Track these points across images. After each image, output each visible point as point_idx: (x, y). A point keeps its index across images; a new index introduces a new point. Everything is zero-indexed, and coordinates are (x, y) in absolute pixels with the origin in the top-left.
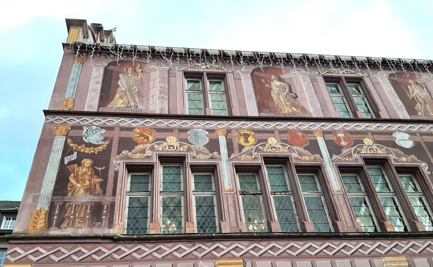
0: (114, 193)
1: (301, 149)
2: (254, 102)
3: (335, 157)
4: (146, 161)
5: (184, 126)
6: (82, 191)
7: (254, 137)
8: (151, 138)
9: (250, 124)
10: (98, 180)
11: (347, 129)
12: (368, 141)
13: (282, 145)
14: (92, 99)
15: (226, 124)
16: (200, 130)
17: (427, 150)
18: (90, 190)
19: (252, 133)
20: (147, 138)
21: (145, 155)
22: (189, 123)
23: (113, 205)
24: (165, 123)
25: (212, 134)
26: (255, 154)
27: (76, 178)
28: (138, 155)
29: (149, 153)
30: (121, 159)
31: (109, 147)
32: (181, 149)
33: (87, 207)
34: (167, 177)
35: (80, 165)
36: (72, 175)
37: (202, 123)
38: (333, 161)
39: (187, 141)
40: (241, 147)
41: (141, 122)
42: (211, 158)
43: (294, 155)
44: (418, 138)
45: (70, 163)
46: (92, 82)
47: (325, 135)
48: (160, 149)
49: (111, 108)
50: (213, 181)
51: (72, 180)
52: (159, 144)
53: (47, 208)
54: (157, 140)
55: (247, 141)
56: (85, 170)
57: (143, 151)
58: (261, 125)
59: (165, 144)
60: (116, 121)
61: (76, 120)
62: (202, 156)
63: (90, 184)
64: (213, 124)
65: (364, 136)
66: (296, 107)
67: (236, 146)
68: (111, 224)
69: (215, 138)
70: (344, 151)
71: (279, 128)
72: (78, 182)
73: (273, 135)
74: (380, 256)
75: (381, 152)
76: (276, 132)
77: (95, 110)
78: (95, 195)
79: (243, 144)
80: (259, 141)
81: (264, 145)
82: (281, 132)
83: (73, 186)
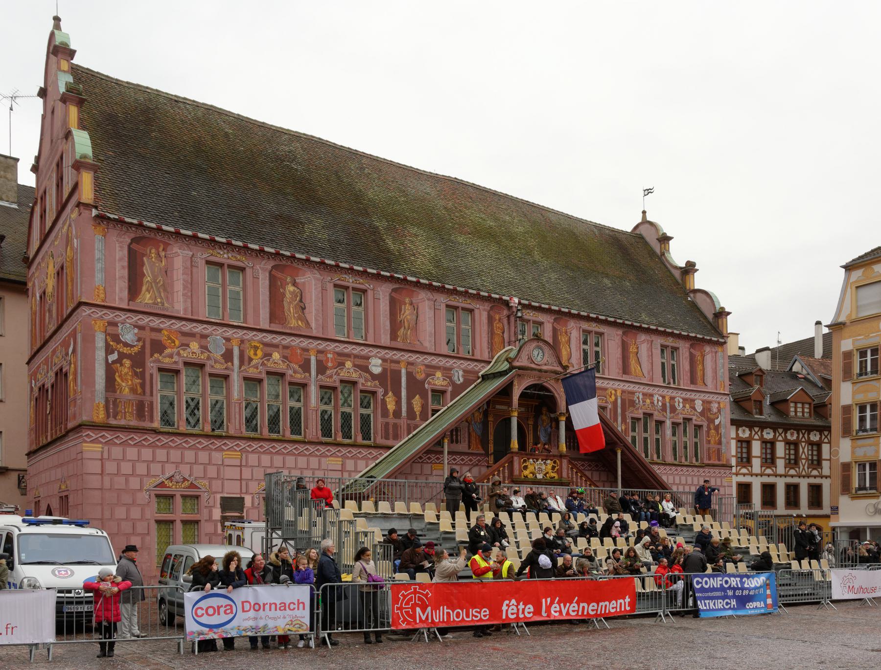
0: (152, 395)
1: (296, 367)
2: (268, 310)
3: (320, 376)
4: (174, 367)
5: (205, 332)
6: (127, 390)
7: (262, 351)
8: (177, 343)
9: (260, 335)
10: (138, 381)
11: (337, 350)
12: (349, 364)
13: (282, 361)
15: (241, 333)
16: (218, 337)
17: (389, 378)
18: (133, 390)
19: (261, 346)
20: (174, 342)
21: (173, 360)
22: (210, 329)
25: (228, 343)
27: (120, 376)
28: (167, 360)
29: (176, 358)
30: (154, 362)
32: (202, 357)
33: (133, 404)
34: (188, 378)
35: (122, 365)
36: (117, 374)
37: (221, 330)
38: (317, 381)
39: (206, 348)
40: (251, 360)
42: (226, 368)
43: (290, 372)
44: (388, 365)
45: (114, 362)
47: (318, 355)
48: (185, 355)
50: (224, 386)
51: (118, 379)
52: (184, 350)
53: (103, 402)
54: (182, 345)
55: (255, 354)
56: (126, 370)
57: (171, 356)
58: (269, 338)
59: (189, 350)
62: (218, 366)
63: (132, 384)
64: (230, 332)
65: (347, 359)
66: (302, 321)
67: (246, 358)
69: (230, 347)
70: (328, 372)
71: (284, 343)
72: (123, 382)
73: (277, 349)
75: (354, 376)
76: (280, 346)
78: (137, 394)
79: (252, 356)
81: (268, 360)
82: (285, 347)
83: (119, 385)
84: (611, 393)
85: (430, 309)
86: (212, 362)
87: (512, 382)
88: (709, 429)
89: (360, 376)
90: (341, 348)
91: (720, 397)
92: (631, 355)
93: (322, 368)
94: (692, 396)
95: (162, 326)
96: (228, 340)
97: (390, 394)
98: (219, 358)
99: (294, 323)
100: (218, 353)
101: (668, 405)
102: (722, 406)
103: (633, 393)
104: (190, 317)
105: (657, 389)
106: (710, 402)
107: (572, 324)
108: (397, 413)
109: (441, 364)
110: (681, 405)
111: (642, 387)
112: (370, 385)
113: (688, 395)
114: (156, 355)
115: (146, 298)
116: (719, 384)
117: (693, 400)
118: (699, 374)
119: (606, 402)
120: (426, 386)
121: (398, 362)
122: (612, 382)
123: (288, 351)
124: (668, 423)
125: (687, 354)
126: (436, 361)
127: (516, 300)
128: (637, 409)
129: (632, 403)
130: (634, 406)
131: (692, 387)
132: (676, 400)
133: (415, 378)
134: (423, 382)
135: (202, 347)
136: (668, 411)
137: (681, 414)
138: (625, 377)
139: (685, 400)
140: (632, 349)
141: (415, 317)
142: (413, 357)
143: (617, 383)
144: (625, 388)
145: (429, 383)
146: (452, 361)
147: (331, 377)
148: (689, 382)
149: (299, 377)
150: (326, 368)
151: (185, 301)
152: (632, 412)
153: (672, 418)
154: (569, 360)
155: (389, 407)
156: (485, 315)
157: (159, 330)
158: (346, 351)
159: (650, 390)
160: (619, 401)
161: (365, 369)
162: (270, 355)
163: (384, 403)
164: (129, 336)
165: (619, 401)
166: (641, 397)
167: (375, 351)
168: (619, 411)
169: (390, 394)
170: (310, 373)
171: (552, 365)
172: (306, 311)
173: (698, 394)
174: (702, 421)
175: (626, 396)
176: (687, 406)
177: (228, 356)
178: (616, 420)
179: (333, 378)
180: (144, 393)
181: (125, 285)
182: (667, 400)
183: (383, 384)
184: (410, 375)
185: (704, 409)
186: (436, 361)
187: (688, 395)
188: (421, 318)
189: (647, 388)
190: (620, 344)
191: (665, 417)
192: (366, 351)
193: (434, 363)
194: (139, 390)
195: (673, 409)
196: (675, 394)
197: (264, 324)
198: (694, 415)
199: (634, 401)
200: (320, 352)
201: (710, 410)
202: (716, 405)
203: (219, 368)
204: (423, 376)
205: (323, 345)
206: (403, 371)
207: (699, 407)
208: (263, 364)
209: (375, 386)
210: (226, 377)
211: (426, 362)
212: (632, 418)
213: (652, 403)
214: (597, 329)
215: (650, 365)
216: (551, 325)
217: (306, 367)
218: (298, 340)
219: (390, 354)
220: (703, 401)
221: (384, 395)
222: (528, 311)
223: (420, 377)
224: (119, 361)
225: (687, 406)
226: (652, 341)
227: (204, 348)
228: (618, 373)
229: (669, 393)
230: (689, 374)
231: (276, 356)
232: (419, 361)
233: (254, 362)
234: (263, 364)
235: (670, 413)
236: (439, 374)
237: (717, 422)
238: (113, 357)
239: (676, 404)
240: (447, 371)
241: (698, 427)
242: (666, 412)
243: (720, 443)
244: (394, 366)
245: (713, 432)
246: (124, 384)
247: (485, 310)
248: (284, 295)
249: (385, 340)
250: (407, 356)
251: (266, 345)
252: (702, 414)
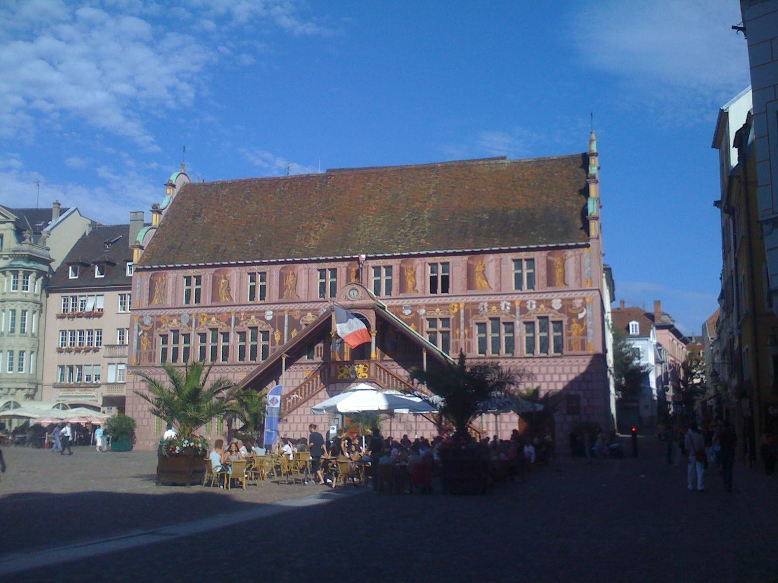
0: (155, 348)
1: (224, 324)
4: (166, 333)
5: (180, 313)
6: (145, 348)
8: (167, 321)
9: (206, 309)
11: (247, 310)
12: (253, 317)
14: (146, 300)
18: (148, 348)
23: (155, 353)
24: (172, 312)
26: (205, 327)
28: (162, 330)
31: (153, 326)
37: (187, 310)
39: (180, 321)
40: (201, 323)
41: (164, 311)
42: (189, 330)
44: (276, 314)
46: (145, 289)
49: (153, 305)
51: (142, 343)
55: (203, 320)
57: (164, 328)
58: (210, 310)
60: (155, 312)
61: (141, 313)
64: (192, 311)
68: (154, 362)
70: (241, 324)
71: (218, 311)
74: (238, 372)
77: (147, 307)
80: (208, 320)
82: (219, 314)
84: (454, 306)
85: (305, 274)
86: (182, 328)
87: (330, 317)
88: (570, 322)
89: (259, 322)
90: (249, 308)
91: (586, 293)
92: (477, 274)
93: (237, 322)
94: (550, 296)
95: (162, 314)
96: (190, 315)
97: (277, 330)
98: (186, 325)
99: (224, 299)
100: (185, 324)
101: (518, 308)
102: (588, 300)
103: (478, 303)
104: (174, 307)
105: (505, 296)
106: (571, 299)
107: (418, 261)
108: (281, 342)
109: (312, 307)
110: (534, 306)
111: (487, 297)
112: (265, 328)
113: (544, 296)
114: (158, 329)
115: (156, 301)
116: (584, 281)
117: (550, 300)
118: (558, 276)
119: (449, 314)
120: (301, 323)
121: (283, 311)
122: (454, 298)
123: (220, 315)
124: (517, 323)
125: (544, 262)
126: (307, 306)
127: (364, 256)
128: (483, 315)
129: (476, 312)
130: (478, 314)
131: (550, 289)
132: (529, 302)
133: (294, 319)
134: (299, 320)
135: (178, 321)
136: (518, 313)
137: (534, 313)
138: (470, 292)
139: (539, 302)
140: (479, 269)
141: (295, 281)
142: (292, 306)
143: (460, 298)
144: (468, 301)
145: (303, 321)
146: (319, 304)
147: (242, 326)
148: (545, 285)
149: (225, 330)
150: (240, 321)
151: (172, 300)
152: (475, 319)
153: (524, 318)
154: (414, 288)
155: (276, 339)
156: (344, 270)
157: (160, 316)
158: (252, 310)
159: (498, 298)
160: (462, 312)
161: (263, 318)
162: (211, 319)
163: (273, 336)
164: (147, 321)
165: (462, 312)
166: (486, 305)
167: (269, 306)
168: (462, 319)
169: (277, 330)
170: (231, 326)
171: (365, 299)
172: (231, 292)
173: (556, 295)
174: (560, 317)
175: (469, 307)
176: (542, 306)
177: (190, 324)
178: (458, 326)
179: (244, 327)
180: (152, 348)
181: (147, 297)
182: (517, 304)
183: (273, 326)
184: (289, 317)
185: (563, 307)
186: (307, 306)
187: (544, 296)
188: (299, 281)
189: (493, 297)
190: (465, 268)
191: (513, 318)
192: (263, 307)
193: (306, 308)
194: (150, 347)
195: (524, 310)
196: (526, 297)
197: (209, 303)
198: (550, 313)
199: (478, 310)
200: (237, 313)
201: (571, 306)
202: (580, 301)
203: (185, 331)
204: (299, 316)
205: (239, 309)
206: (286, 316)
207: (557, 304)
208: (207, 325)
209: (268, 328)
210: (189, 334)
211: (301, 308)
212: (477, 324)
213: (499, 308)
214: (442, 261)
215: (498, 279)
216: (398, 266)
217: (229, 323)
218: (225, 308)
219: (278, 307)
220: (563, 300)
221: (273, 332)
222: (380, 260)
223: (297, 317)
224: (143, 334)
225: (542, 306)
226: (501, 259)
227: (179, 321)
228: (463, 290)
229: (518, 299)
230: (545, 279)
231: (214, 319)
232: (296, 308)
233: (202, 325)
234: (207, 325)
235: (520, 314)
236: (310, 314)
237: (581, 316)
238: (141, 333)
239: (528, 307)
240: (315, 311)
241: (558, 324)
242: (515, 314)
243: (585, 333)
244: (281, 314)
245: (575, 325)
246: (144, 345)
247: (343, 267)
248: (219, 286)
249: (275, 299)
250: (289, 306)
251: (208, 314)
252: (561, 311)
